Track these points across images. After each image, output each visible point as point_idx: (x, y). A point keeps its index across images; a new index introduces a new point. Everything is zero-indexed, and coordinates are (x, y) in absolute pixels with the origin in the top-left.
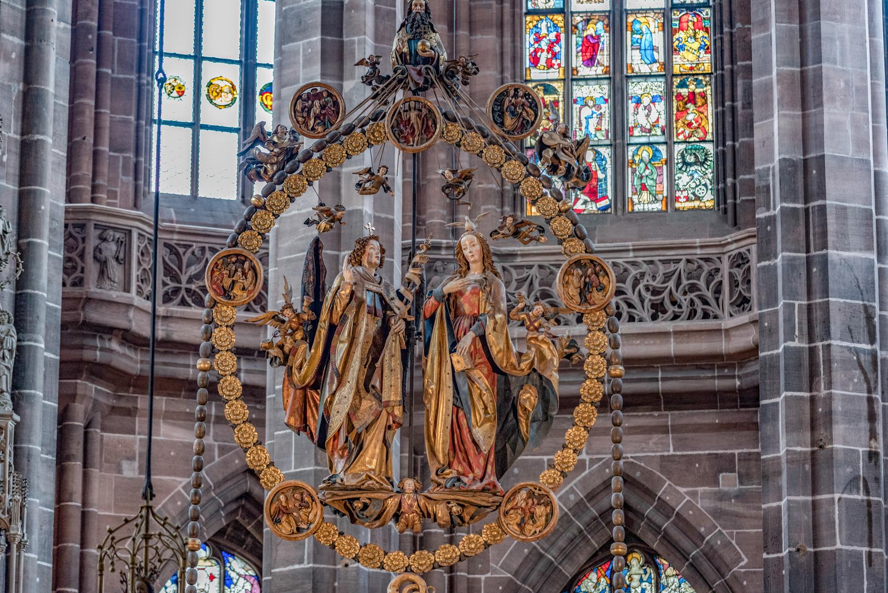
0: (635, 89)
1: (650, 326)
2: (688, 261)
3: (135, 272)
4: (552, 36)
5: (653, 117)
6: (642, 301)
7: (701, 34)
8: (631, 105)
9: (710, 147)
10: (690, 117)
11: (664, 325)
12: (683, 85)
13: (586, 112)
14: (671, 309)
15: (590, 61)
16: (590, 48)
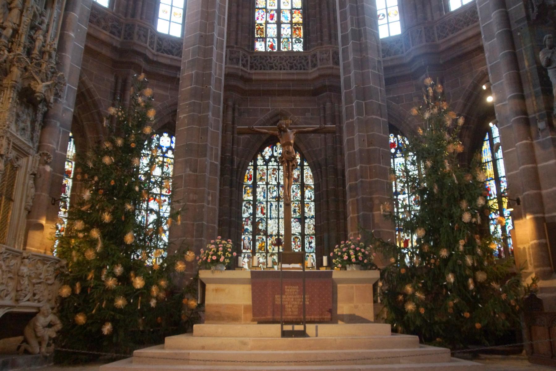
0: (282, 25)
1: (290, 71)
2: (300, 57)
3: (148, 40)
4: (262, 13)
5: (287, 33)
6: (287, 65)
7: (300, 15)
8: (282, 29)
9: (302, 40)
10: (297, 32)
11: (292, 71)
12: (295, 25)
13: (271, 30)
14: (295, 68)
15: (272, 19)
16: (272, 17)
